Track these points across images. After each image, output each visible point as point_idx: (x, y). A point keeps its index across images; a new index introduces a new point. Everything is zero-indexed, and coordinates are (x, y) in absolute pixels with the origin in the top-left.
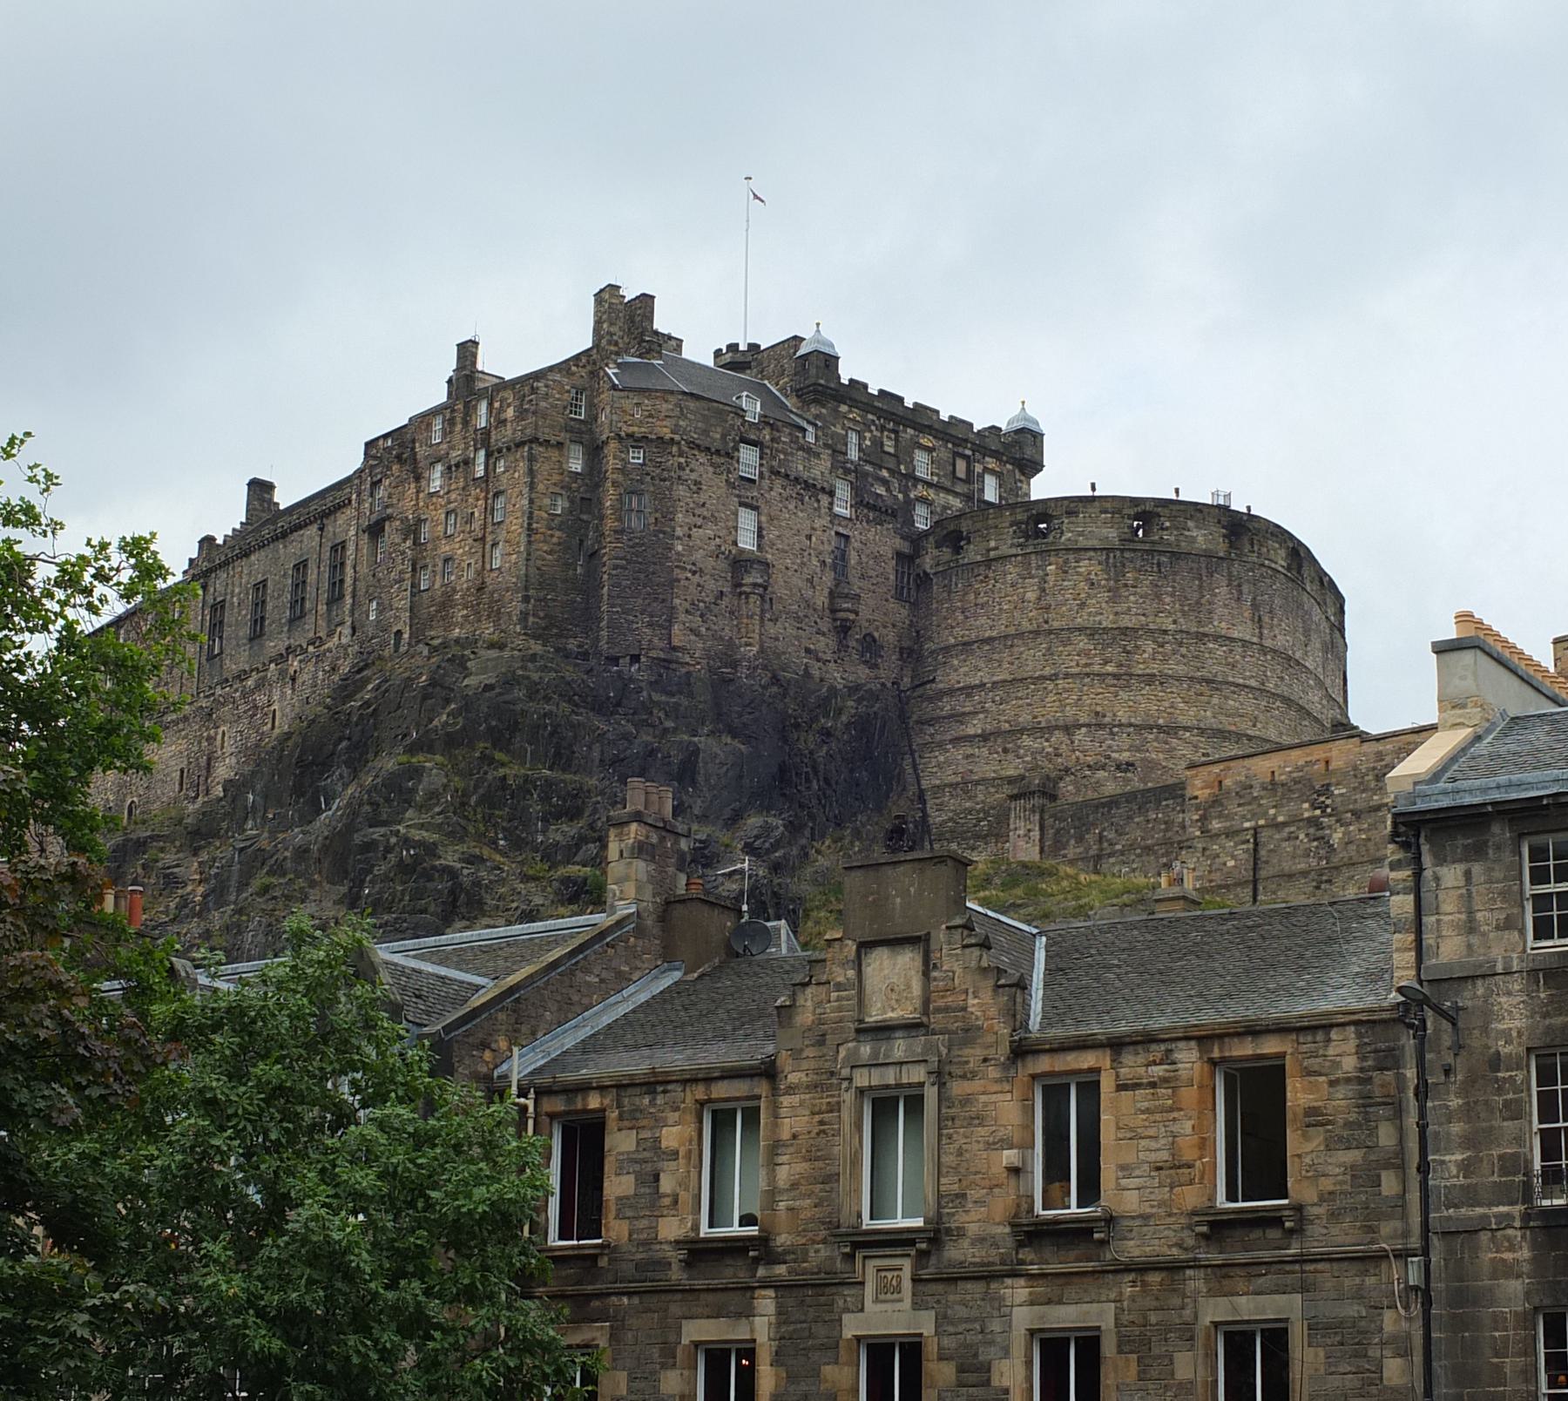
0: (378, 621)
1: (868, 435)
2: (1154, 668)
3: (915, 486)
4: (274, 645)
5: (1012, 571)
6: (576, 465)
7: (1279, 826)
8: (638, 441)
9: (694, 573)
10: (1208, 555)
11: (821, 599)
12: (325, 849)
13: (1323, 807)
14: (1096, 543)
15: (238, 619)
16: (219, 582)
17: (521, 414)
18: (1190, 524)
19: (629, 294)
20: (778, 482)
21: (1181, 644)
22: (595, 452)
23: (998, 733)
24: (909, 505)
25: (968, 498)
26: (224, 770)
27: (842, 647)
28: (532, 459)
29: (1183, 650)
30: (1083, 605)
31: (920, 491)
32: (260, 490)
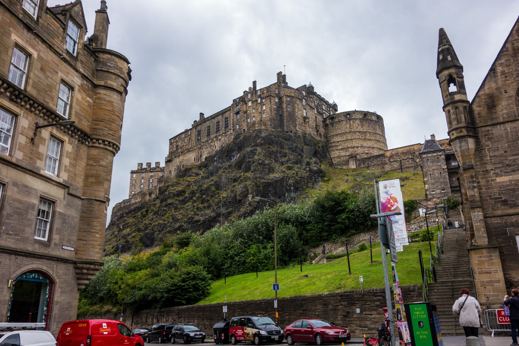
0: (239, 129)
2: (370, 138)
4: (212, 136)
5: (344, 123)
6: (277, 101)
7: (405, 160)
8: (289, 96)
11: (314, 126)
12: (236, 165)
13: (414, 156)
15: (204, 133)
16: (199, 128)
17: (268, 92)
19: (283, 74)
22: (280, 98)
23: (344, 148)
26: (204, 157)
27: (317, 134)
28: (270, 99)
32: (202, 114)
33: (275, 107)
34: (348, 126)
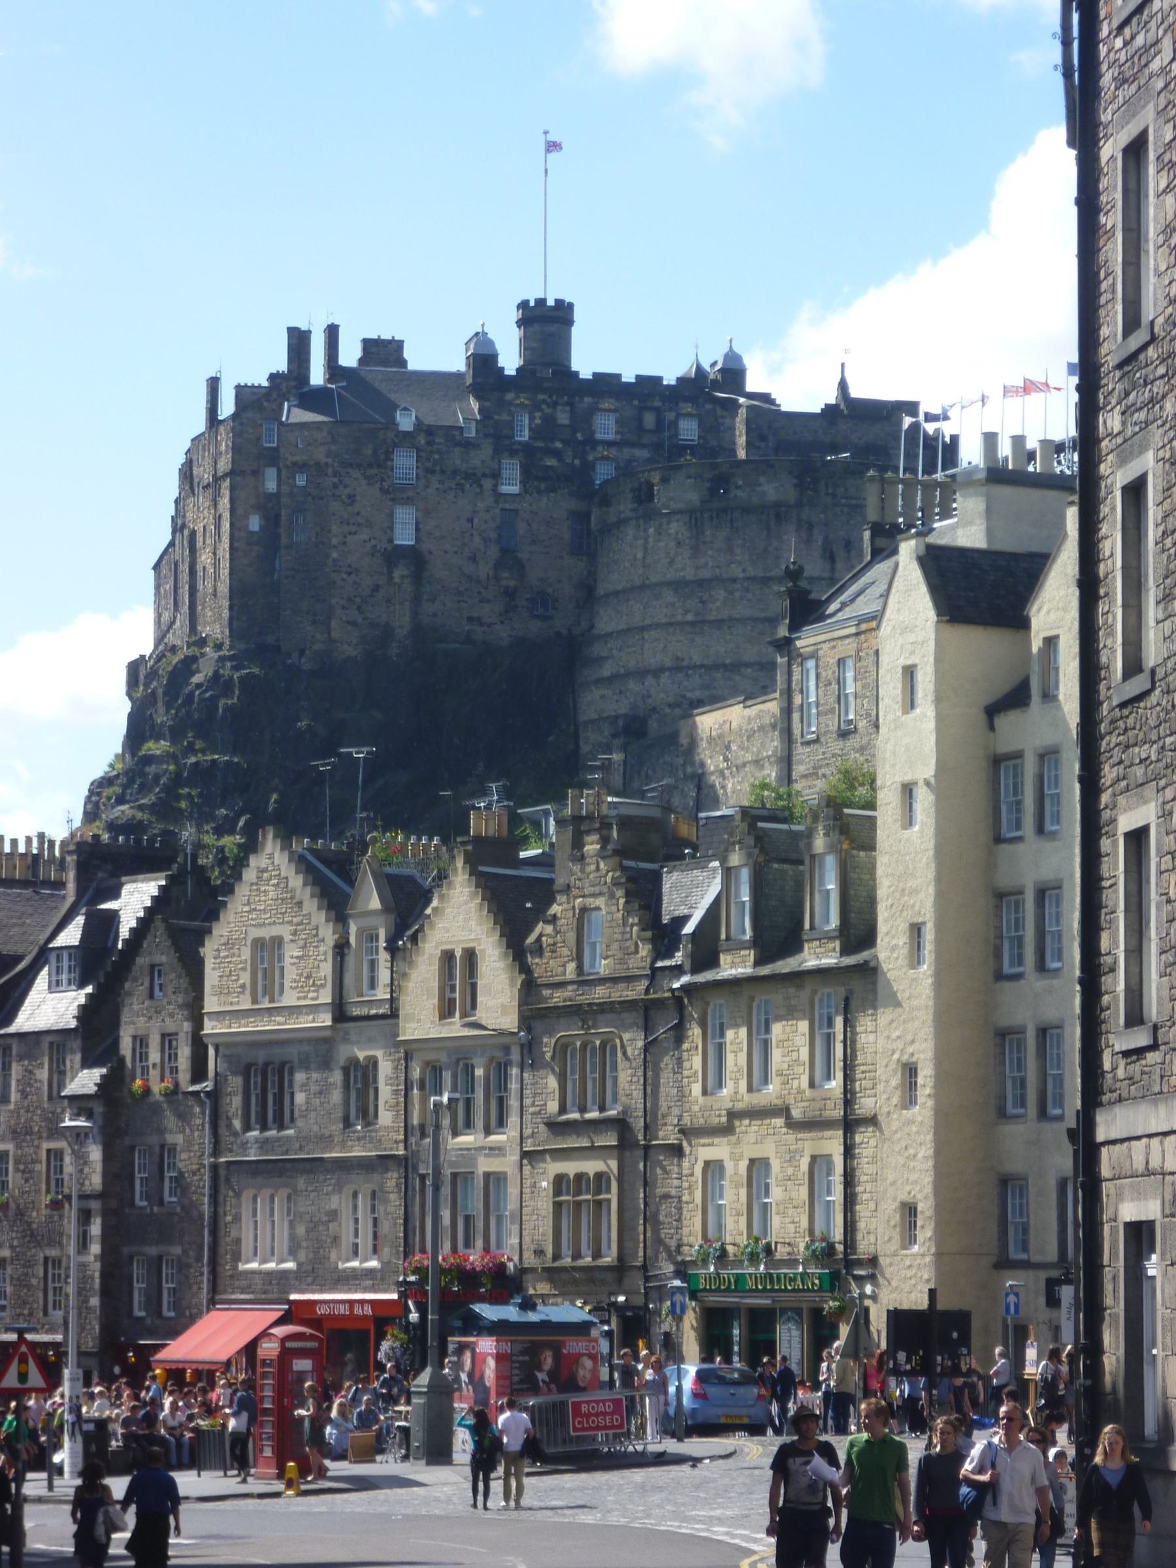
1: (538, 414)
2: (725, 613)
3: (594, 449)
5: (630, 531)
8: (301, 467)
9: (350, 574)
10: (777, 505)
11: (484, 570)
14: (681, 506)
18: (762, 479)
20: (434, 481)
21: (747, 590)
24: (588, 468)
25: (657, 447)
29: (749, 596)
30: (671, 563)
31: (601, 451)
33: (255, 523)
34: (640, 555)
